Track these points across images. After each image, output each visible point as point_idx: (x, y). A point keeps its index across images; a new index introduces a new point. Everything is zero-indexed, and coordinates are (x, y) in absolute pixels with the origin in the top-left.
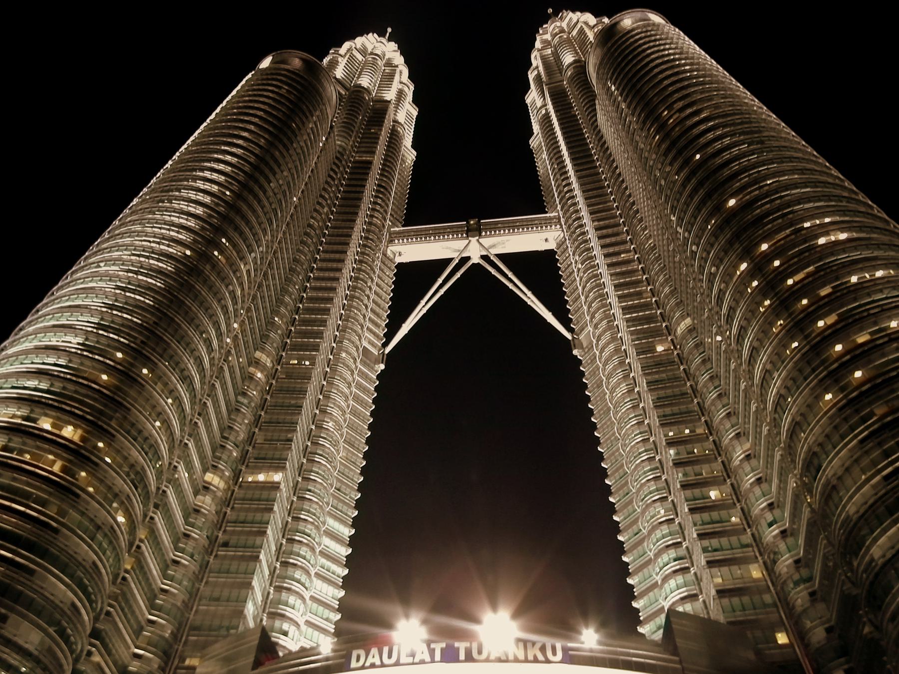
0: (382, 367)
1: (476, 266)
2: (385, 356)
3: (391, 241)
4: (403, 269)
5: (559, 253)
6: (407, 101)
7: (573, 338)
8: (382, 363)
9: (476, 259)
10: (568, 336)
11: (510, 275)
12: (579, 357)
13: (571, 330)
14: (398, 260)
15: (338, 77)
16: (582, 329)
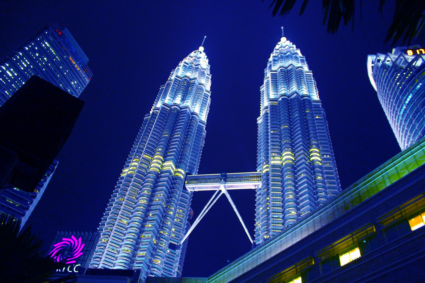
9: (224, 191)
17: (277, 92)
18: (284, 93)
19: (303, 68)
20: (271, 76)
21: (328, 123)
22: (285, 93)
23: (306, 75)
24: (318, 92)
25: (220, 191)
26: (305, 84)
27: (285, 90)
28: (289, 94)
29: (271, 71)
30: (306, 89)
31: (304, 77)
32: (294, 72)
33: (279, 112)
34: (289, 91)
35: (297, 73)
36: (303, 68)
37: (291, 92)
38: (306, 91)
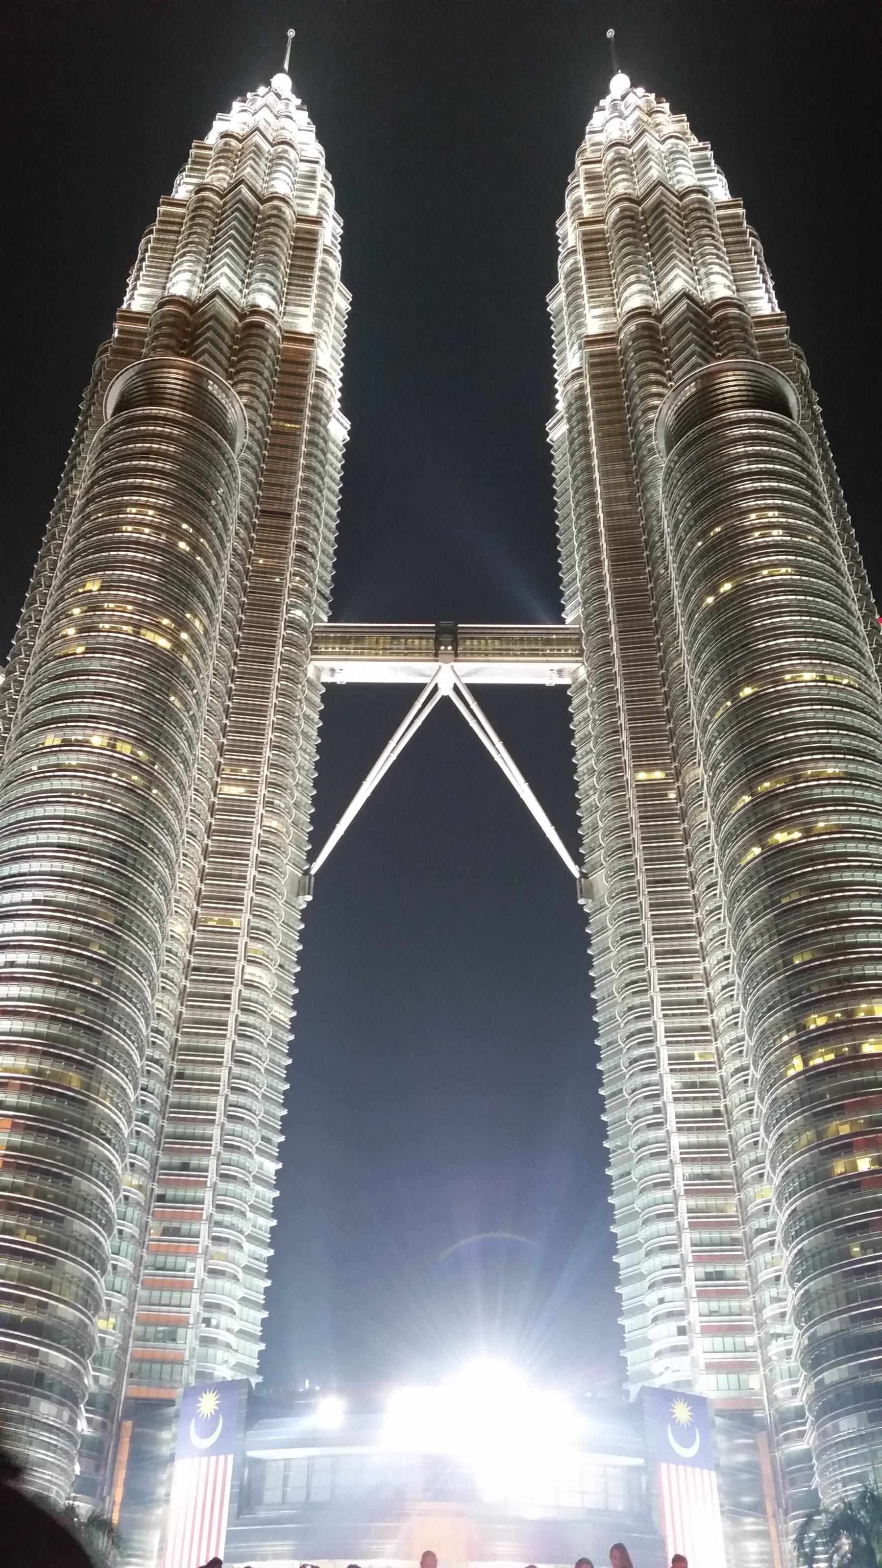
0: (309, 898)
1: (446, 700)
2: (313, 879)
3: (314, 651)
4: (332, 689)
5: (575, 702)
6: (336, 289)
7: (584, 876)
8: (309, 894)
10: (575, 870)
11: (499, 745)
12: (586, 910)
13: (579, 860)
14: (326, 678)
15: (223, 284)
16: (594, 868)
17: (614, 305)
18: (639, 304)
19: (706, 194)
20: (585, 242)
21: (819, 403)
22: (647, 303)
23: (720, 219)
24: (771, 284)
25: (435, 689)
26: (718, 257)
27: (641, 291)
28: (658, 304)
29: (581, 224)
30: (723, 275)
31: (712, 229)
32: (674, 214)
33: (628, 385)
34: (660, 293)
35: (685, 218)
36: (706, 194)
37: (664, 298)
38: (725, 286)
